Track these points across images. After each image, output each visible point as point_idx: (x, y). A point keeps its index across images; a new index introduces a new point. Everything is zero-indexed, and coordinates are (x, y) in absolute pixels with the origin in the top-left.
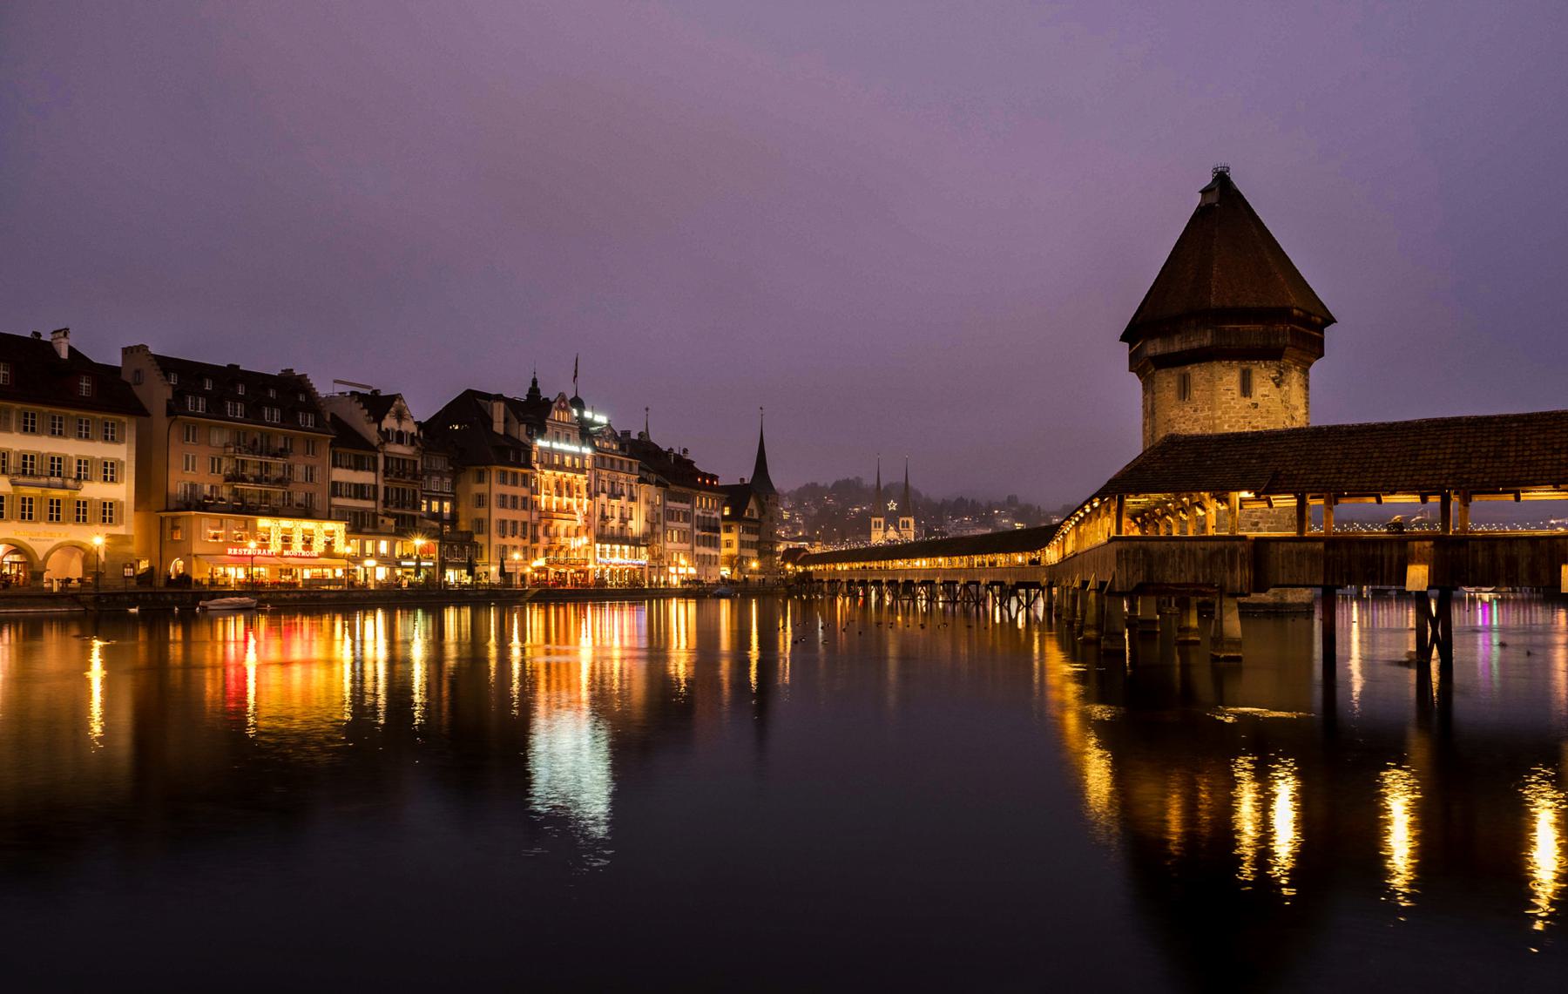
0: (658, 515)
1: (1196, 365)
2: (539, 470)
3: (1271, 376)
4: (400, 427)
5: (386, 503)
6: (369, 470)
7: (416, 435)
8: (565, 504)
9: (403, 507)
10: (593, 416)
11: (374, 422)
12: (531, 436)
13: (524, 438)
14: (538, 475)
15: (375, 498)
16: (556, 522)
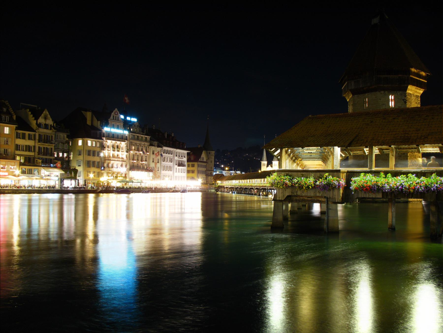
0: (158, 160)
1: (369, 93)
2: (105, 140)
3: (402, 98)
4: (46, 122)
5: (39, 153)
6: (32, 139)
7: (52, 125)
8: (116, 155)
9: (46, 155)
10: (125, 118)
11: (35, 119)
12: (102, 126)
13: (99, 127)
14: (105, 142)
15: (34, 151)
16: (112, 162)
